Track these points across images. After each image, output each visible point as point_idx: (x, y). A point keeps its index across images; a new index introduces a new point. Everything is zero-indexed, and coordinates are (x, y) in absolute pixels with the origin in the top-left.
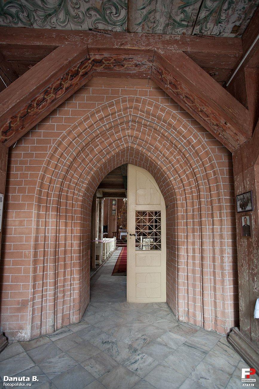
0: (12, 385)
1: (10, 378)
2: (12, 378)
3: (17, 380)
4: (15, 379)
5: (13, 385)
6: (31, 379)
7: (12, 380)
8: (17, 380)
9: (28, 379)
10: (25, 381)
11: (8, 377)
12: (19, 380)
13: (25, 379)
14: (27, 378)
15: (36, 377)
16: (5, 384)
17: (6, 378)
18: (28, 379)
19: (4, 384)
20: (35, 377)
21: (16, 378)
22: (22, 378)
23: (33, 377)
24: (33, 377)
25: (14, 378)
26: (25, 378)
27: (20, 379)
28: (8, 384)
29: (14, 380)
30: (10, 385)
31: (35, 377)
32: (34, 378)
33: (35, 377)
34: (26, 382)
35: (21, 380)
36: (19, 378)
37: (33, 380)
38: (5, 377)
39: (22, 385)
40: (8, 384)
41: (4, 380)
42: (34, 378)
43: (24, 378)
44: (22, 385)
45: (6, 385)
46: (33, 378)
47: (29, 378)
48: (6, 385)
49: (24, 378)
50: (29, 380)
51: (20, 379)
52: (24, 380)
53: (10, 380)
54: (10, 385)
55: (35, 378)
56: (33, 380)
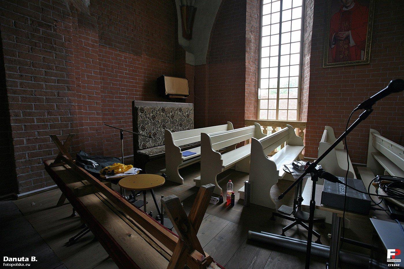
0: (12, 265)
1: (10, 258)
2: (11, 259)
3: (16, 261)
4: (15, 260)
5: (13, 265)
6: (30, 259)
7: (12, 261)
8: (16, 261)
9: (27, 259)
10: (24, 261)
11: (7, 258)
12: (19, 260)
13: (24, 259)
14: (26, 258)
15: (35, 257)
16: (4, 265)
17: (6, 259)
18: (27, 259)
19: (4, 264)
20: (33, 258)
21: (16, 259)
22: (21, 258)
23: (32, 257)
24: (32, 257)
25: (14, 259)
26: (24, 258)
27: (20, 259)
28: (8, 264)
29: (13, 261)
30: (10, 265)
31: (33, 257)
32: (33, 259)
33: (33, 258)
34: (25, 263)
35: (21, 260)
36: (18, 258)
37: (32, 260)
38: (4, 257)
39: (21, 265)
40: (8, 264)
41: (4, 260)
42: (33, 259)
43: (23, 258)
44: (21, 265)
45: (6, 265)
46: (32, 259)
47: (28, 259)
48: (6, 265)
49: (23, 258)
50: (28, 261)
51: (20, 259)
52: (23, 260)
53: (9, 260)
54: (10, 265)
55: (33, 259)
56: (32, 260)
